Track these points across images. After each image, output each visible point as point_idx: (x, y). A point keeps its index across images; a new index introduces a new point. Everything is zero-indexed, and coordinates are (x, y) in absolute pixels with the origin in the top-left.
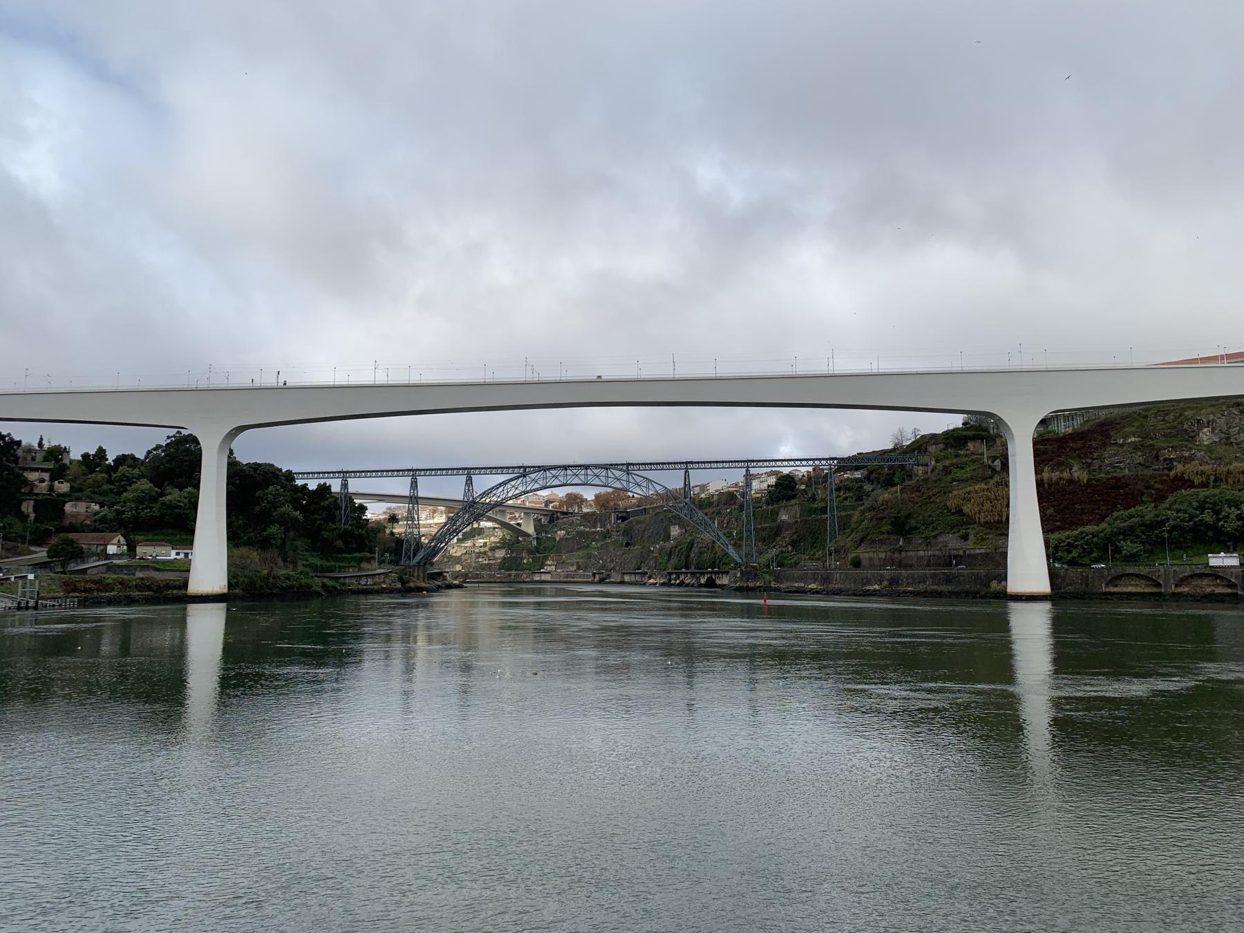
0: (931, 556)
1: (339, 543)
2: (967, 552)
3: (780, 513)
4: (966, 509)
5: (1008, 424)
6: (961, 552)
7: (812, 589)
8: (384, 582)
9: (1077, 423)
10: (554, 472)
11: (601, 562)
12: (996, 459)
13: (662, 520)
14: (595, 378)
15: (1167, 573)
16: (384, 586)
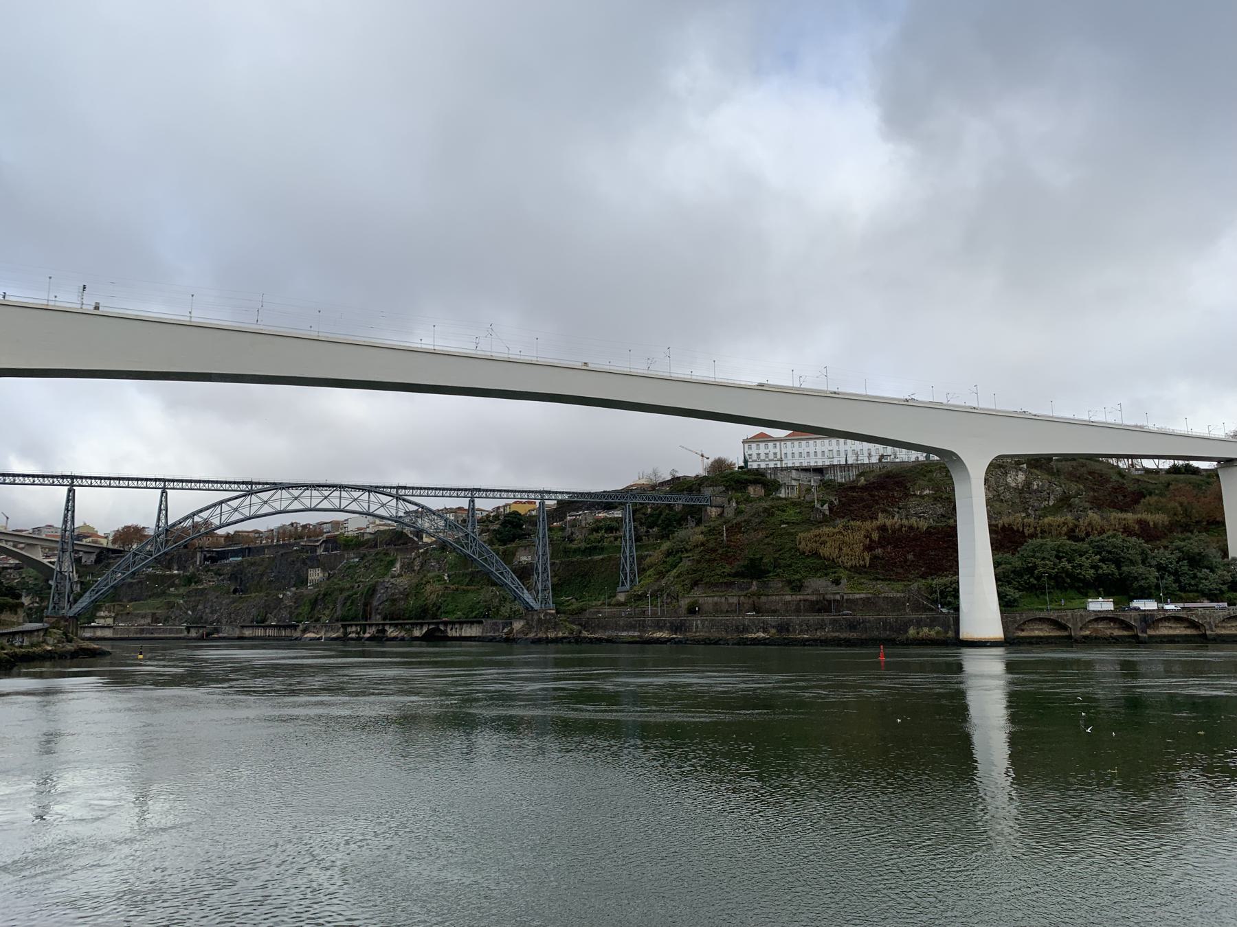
0: (800, 601)
1: (177, 581)
2: (845, 597)
3: (518, 554)
4: (825, 551)
5: (966, 464)
6: (838, 597)
7: (658, 639)
8: (45, 641)
9: (853, 474)
10: (296, 492)
11: (190, 612)
12: (824, 504)
13: (293, 561)
14: (580, 364)
15: (1074, 617)
16: (49, 648)
